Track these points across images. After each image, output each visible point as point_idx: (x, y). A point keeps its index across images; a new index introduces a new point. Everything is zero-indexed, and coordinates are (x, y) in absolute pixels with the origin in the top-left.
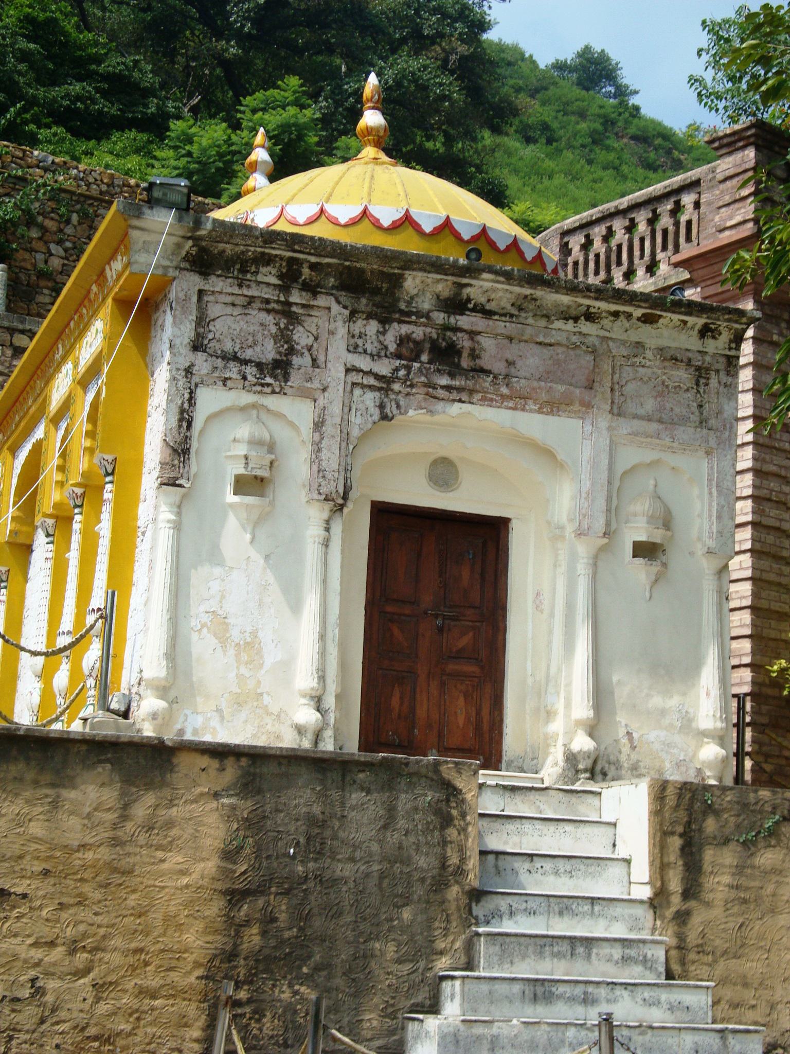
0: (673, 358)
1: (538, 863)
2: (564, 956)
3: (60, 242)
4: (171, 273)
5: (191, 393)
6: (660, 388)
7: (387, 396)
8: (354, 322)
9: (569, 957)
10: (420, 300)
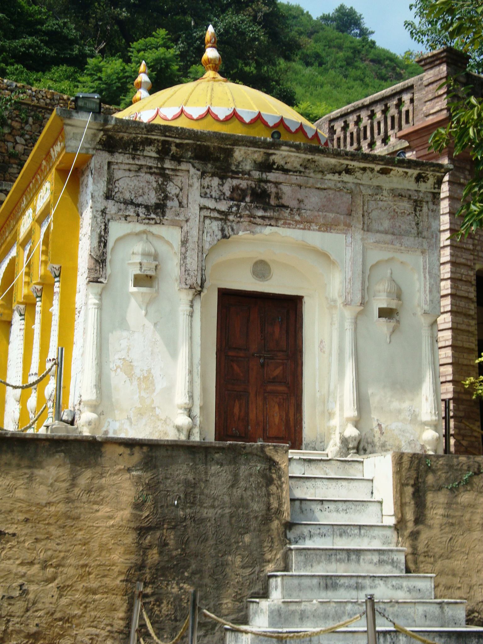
0: (399, 195)
1: (326, 505)
2: (344, 561)
3: (22, 136)
4: (91, 152)
5: (105, 225)
6: (392, 214)
7: (226, 223)
9: (346, 561)
10: (244, 164)
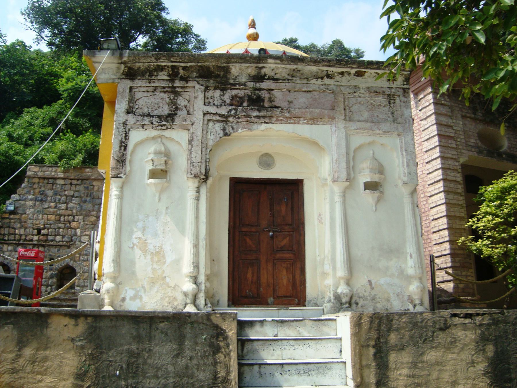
1: (286, 368)
4: (116, 81)
5: (126, 133)
6: (370, 107)
7: (227, 124)
8: (208, 92)
10: (240, 78)
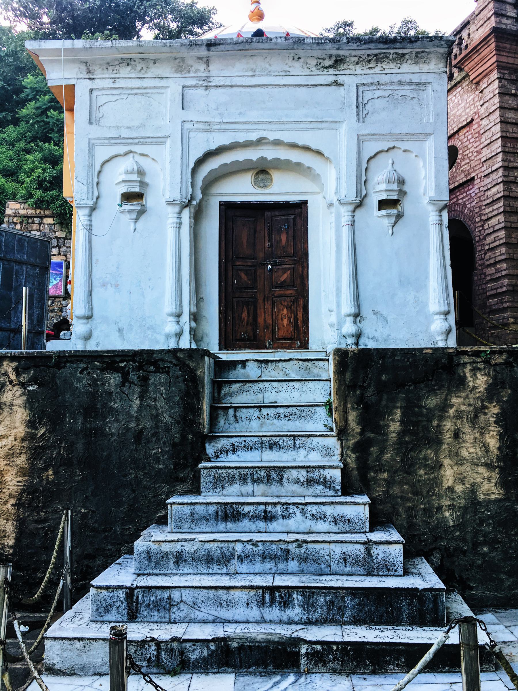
1: (265, 411)
2: (262, 481)
